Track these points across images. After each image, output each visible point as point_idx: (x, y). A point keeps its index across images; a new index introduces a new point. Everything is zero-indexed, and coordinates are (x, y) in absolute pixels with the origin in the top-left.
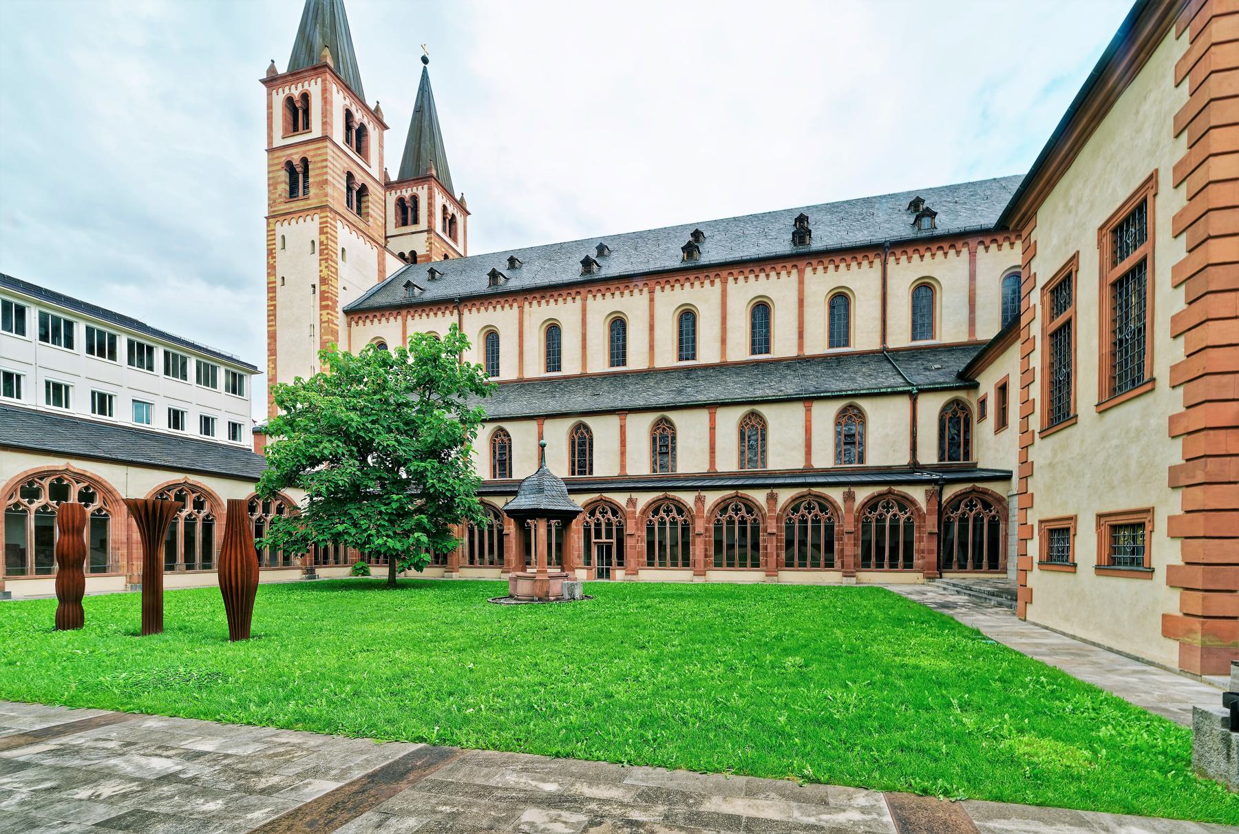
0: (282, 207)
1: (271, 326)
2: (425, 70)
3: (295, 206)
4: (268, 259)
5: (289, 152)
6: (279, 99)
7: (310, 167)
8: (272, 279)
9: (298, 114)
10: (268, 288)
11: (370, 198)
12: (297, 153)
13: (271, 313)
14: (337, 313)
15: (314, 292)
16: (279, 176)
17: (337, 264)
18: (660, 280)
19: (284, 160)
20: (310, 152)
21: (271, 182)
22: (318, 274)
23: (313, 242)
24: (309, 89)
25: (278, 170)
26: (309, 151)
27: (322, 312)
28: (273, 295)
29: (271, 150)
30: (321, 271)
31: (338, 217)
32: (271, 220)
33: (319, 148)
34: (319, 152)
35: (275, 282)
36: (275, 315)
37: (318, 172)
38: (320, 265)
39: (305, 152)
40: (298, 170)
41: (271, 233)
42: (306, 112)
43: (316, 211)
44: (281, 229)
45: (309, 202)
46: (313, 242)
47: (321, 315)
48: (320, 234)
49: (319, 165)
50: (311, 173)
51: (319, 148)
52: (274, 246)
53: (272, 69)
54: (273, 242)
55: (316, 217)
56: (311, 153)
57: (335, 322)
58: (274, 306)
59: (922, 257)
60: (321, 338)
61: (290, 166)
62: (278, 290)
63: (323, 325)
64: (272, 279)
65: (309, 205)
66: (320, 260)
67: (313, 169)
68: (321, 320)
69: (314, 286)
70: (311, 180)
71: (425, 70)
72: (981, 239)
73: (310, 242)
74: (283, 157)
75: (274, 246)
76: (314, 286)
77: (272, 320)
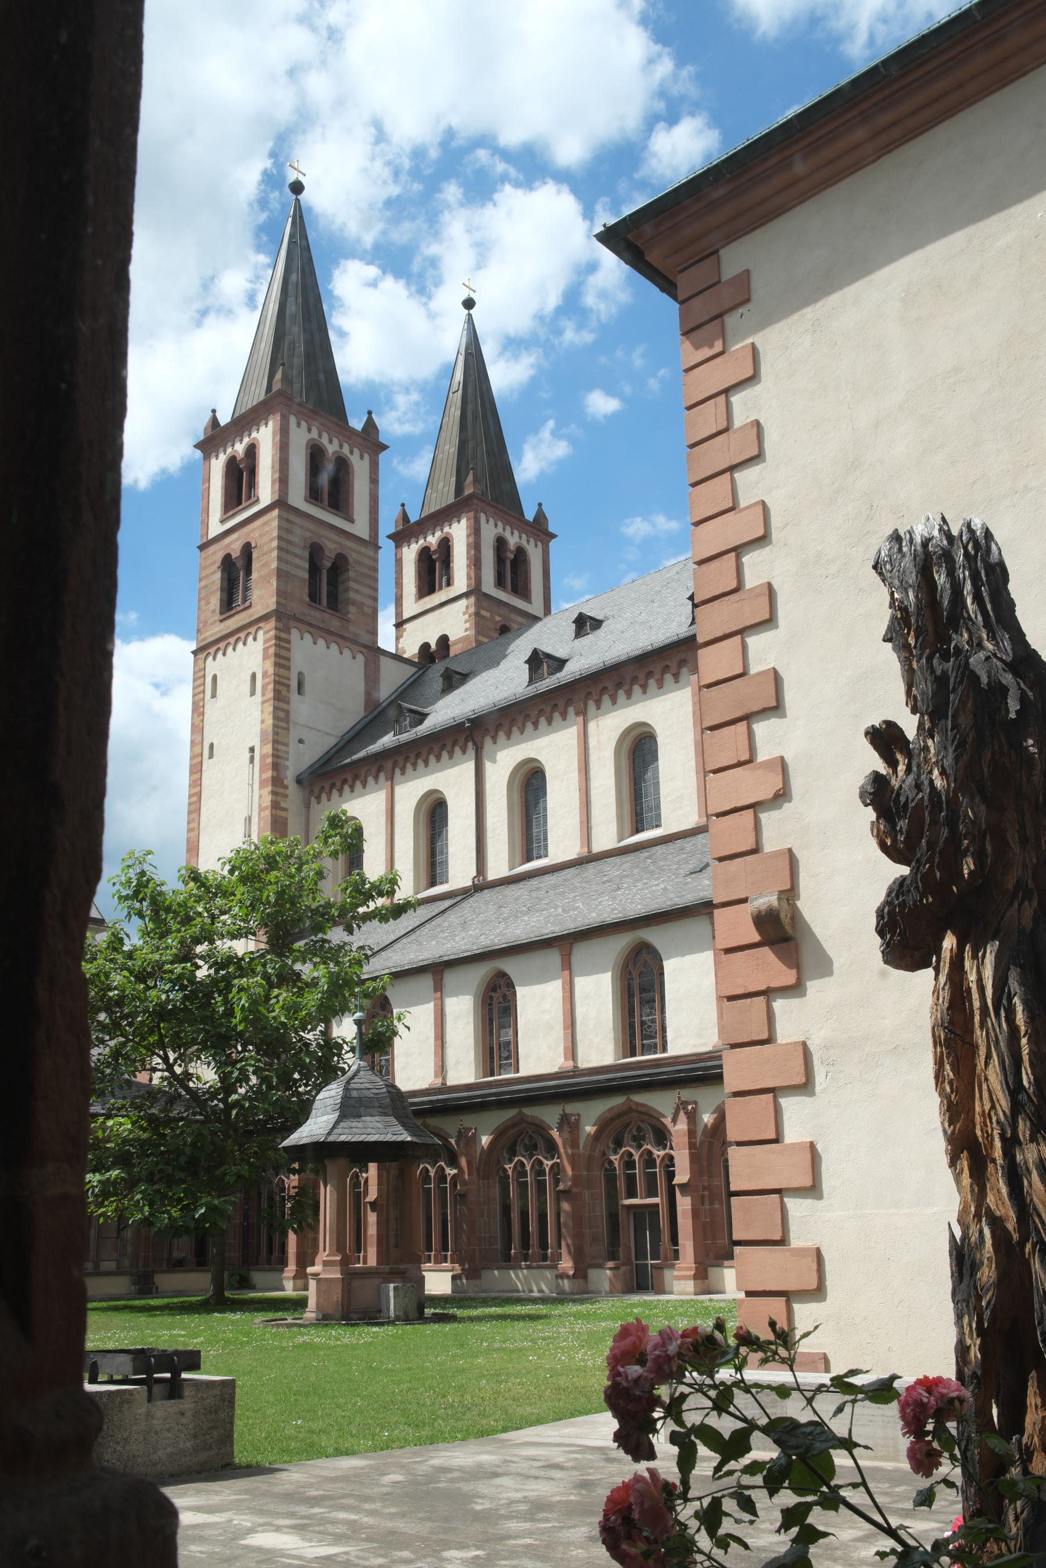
2: (470, 319)
3: (233, 623)
5: (227, 540)
7: (254, 556)
11: (352, 574)
14: (286, 787)
15: (252, 760)
16: (213, 582)
17: (288, 702)
20: (253, 533)
23: (254, 676)
26: (254, 530)
30: (263, 722)
31: (292, 623)
38: (262, 712)
39: (248, 534)
40: (240, 564)
42: (253, 472)
43: (261, 625)
45: (251, 611)
46: (254, 676)
47: (260, 797)
49: (266, 549)
50: (255, 565)
56: (257, 534)
57: (283, 805)
66: (263, 703)
68: (260, 805)
70: (254, 576)
71: (470, 319)
73: (249, 678)
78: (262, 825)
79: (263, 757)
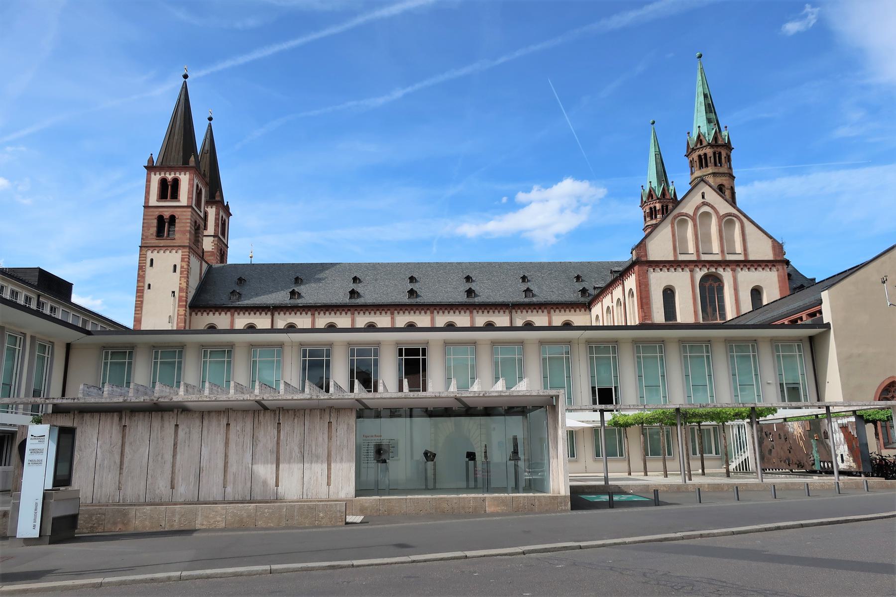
0: (153, 242)
1: (138, 314)
3: (162, 243)
4: (138, 271)
6: (156, 179)
8: (141, 284)
9: (169, 190)
10: (137, 290)
12: (167, 212)
13: (138, 305)
18: (397, 308)
19: (157, 214)
20: (177, 213)
21: (145, 225)
22: (178, 285)
24: (180, 177)
25: (152, 219)
27: (180, 309)
28: (141, 294)
29: (146, 207)
30: (180, 284)
32: (143, 248)
33: (185, 211)
34: (185, 214)
35: (143, 287)
36: (141, 308)
37: (183, 225)
38: (180, 280)
41: (142, 257)
43: (180, 248)
44: (150, 255)
45: (174, 241)
47: (178, 310)
48: (181, 261)
49: (184, 221)
51: (185, 211)
52: (144, 264)
53: (151, 160)
54: (144, 262)
55: (180, 252)
58: (142, 302)
59: (527, 312)
60: (177, 325)
61: (160, 219)
62: (145, 292)
63: (179, 317)
64: (141, 284)
65: (175, 243)
66: (180, 277)
67: (179, 223)
68: (178, 313)
69: (173, 292)
72: (552, 307)
74: (157, 213)
75: (144, 264)
76: (173, 292)
77: (138, 310)
78: (179, 320)
79: (180, 297)
